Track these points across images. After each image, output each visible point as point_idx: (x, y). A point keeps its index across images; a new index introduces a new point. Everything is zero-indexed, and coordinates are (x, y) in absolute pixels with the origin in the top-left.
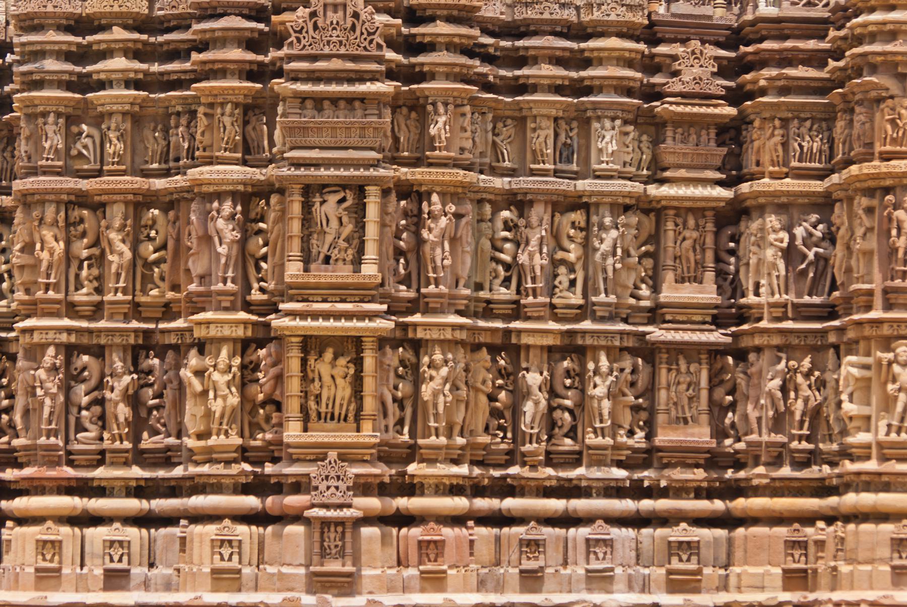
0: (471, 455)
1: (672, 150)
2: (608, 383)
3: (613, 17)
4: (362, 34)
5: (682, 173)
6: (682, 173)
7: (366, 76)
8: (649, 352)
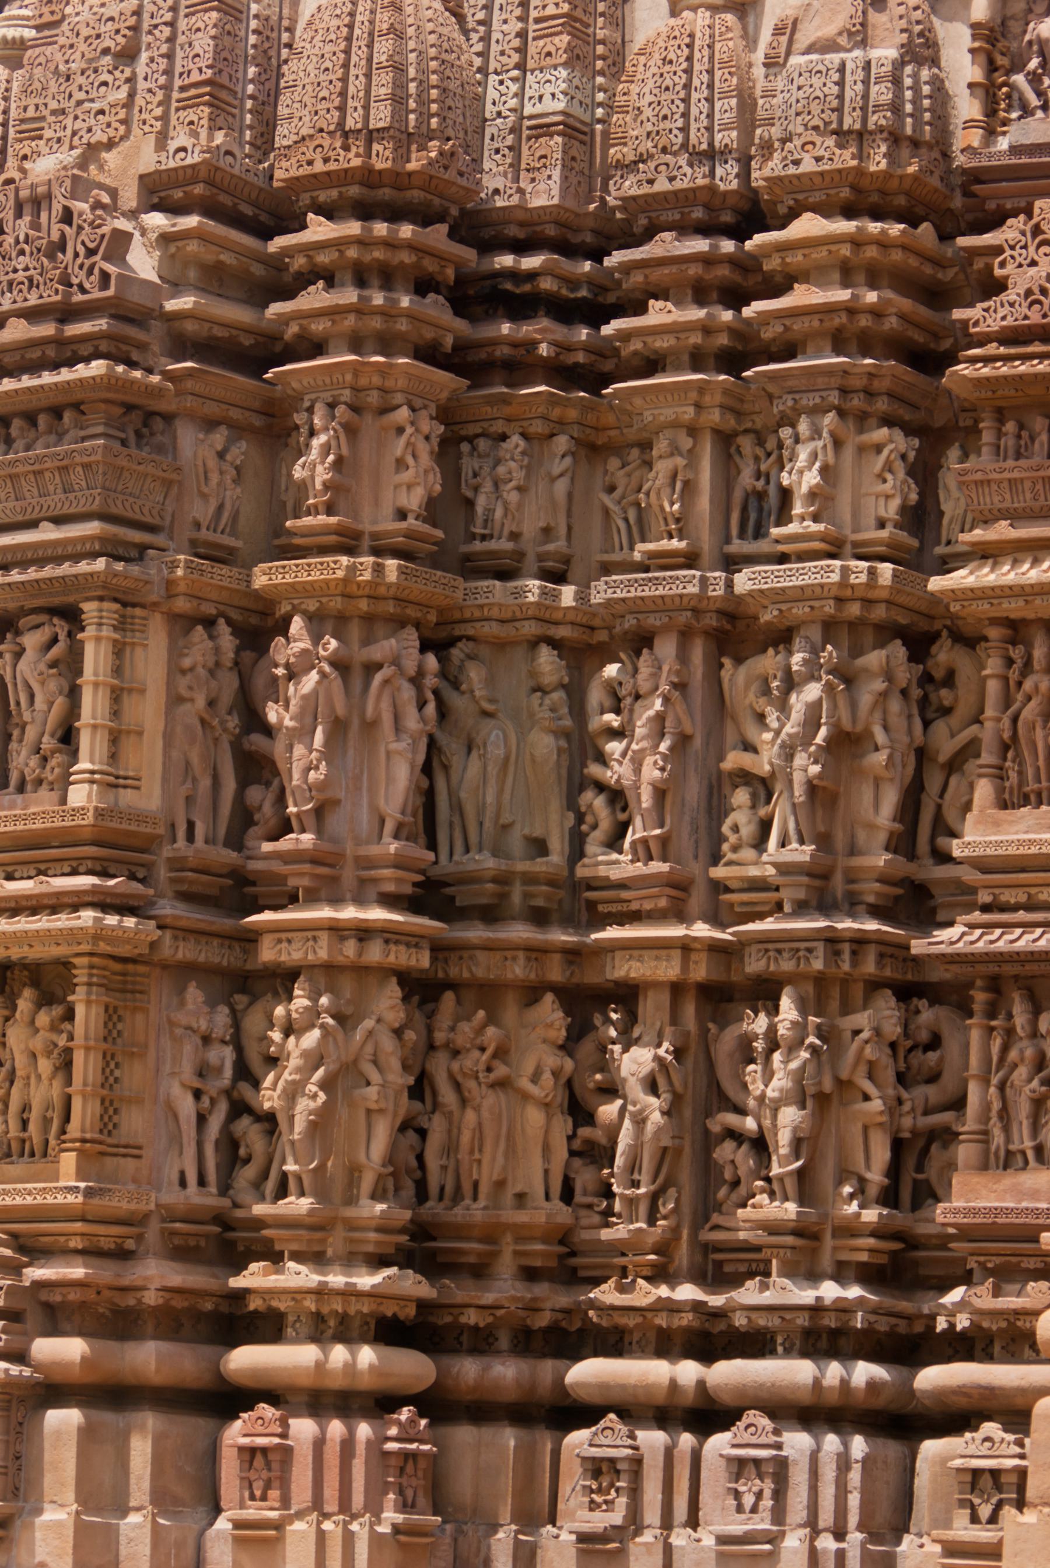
0: (516, 1253)
1: (979, 476)
2: (794, 1065)
3: (808, 165)
4: (76, 255)
5: (1003, 531)
6: (1003, 531)
7: (85, 350)
8: (913, 985)
